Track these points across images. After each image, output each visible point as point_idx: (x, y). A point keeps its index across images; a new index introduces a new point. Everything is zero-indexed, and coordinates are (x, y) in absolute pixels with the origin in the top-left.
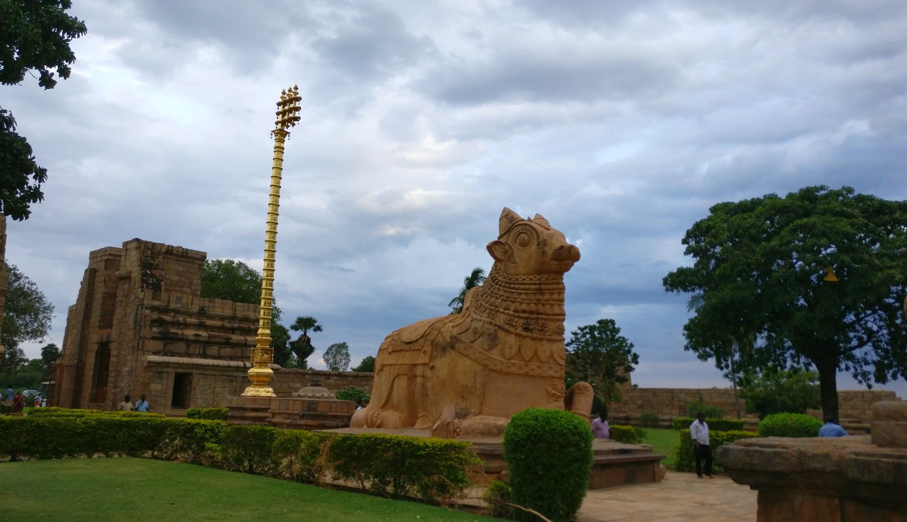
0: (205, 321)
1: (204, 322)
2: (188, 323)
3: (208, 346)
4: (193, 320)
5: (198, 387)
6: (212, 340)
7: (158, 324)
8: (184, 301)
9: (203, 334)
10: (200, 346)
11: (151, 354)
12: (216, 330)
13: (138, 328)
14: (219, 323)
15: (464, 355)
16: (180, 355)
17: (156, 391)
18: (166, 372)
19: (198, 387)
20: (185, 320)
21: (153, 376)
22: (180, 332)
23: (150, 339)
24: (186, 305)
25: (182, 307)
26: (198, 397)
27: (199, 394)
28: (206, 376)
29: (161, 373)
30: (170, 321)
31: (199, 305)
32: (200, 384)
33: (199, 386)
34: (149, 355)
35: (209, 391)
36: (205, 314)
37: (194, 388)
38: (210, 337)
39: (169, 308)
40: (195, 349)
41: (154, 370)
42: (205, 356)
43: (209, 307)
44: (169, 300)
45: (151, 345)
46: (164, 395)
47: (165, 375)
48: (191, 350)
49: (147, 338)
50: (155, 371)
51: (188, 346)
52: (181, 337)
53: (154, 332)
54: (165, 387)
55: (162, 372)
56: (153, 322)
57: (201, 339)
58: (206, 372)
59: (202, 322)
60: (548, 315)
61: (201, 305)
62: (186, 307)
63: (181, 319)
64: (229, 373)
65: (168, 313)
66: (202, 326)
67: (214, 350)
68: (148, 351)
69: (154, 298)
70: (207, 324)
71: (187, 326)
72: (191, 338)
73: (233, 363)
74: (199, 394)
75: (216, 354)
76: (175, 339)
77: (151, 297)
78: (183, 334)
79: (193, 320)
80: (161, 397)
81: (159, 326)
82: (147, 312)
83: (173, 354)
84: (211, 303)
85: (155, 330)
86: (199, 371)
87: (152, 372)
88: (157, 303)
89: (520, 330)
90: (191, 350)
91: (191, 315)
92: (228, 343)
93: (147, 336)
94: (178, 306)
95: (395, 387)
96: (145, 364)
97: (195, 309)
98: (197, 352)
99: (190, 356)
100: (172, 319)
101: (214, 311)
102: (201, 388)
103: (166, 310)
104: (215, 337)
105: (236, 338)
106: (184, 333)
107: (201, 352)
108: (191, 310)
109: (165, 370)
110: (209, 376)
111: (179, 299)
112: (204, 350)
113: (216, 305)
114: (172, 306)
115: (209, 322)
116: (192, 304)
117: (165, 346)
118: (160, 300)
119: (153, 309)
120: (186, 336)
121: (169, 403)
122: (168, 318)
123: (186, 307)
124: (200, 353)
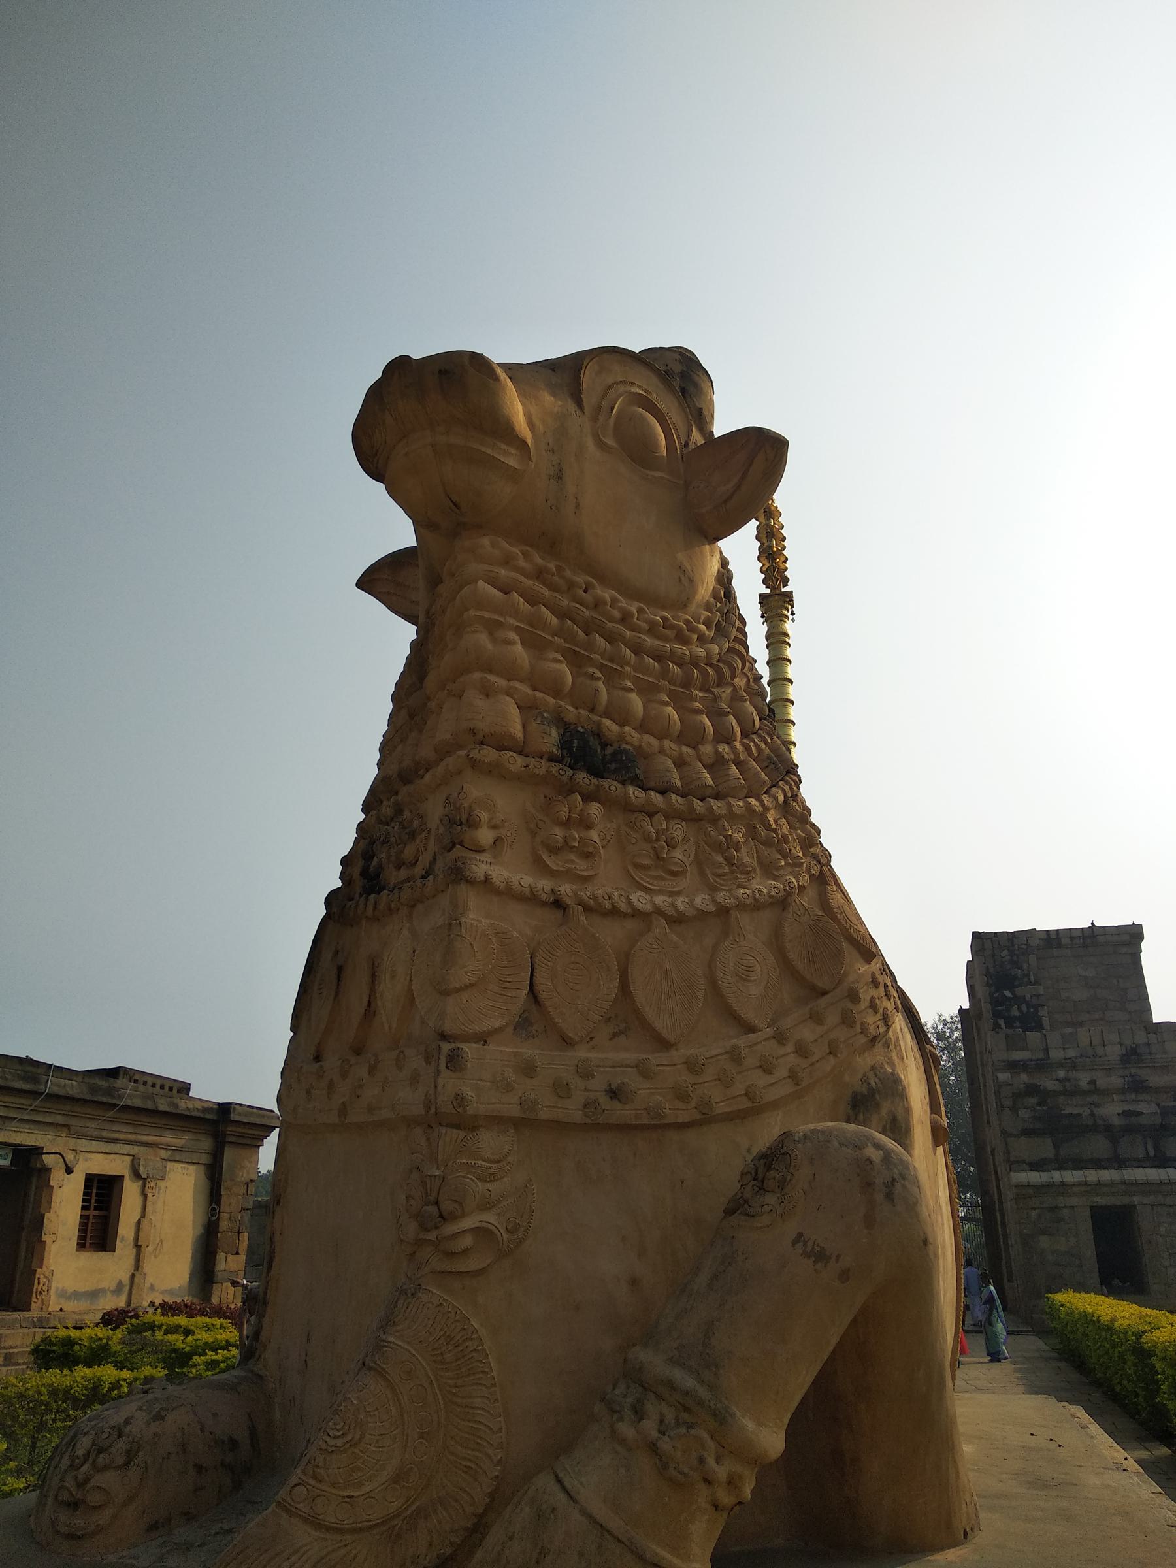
7: (1033, 1101)
11: (1027, 1167)
16: (1098, 1164)
20: (1093, 1082)
25: (1082, 1056)
26: (1167, 1263)
29: (1054, 1209)
43: (1148, 1044)
57: (1144, 1121)
72: (1116, 1122)
78: (1092, 1114)
79: (1116, 1081)
83: (1079, 1164)
88: (1019, 1055)
94: (1071, 1053)
97: (1114, 1052)
98: (1141, 1153)
99: (1120, 1163)
103: (1043, 1065)
107: (1152, 1153)
112: (1156, 1147)
114: (1056, 1055)
117: (1056, 1146)
118: (1025, 1048)
122: (1049, 1084)
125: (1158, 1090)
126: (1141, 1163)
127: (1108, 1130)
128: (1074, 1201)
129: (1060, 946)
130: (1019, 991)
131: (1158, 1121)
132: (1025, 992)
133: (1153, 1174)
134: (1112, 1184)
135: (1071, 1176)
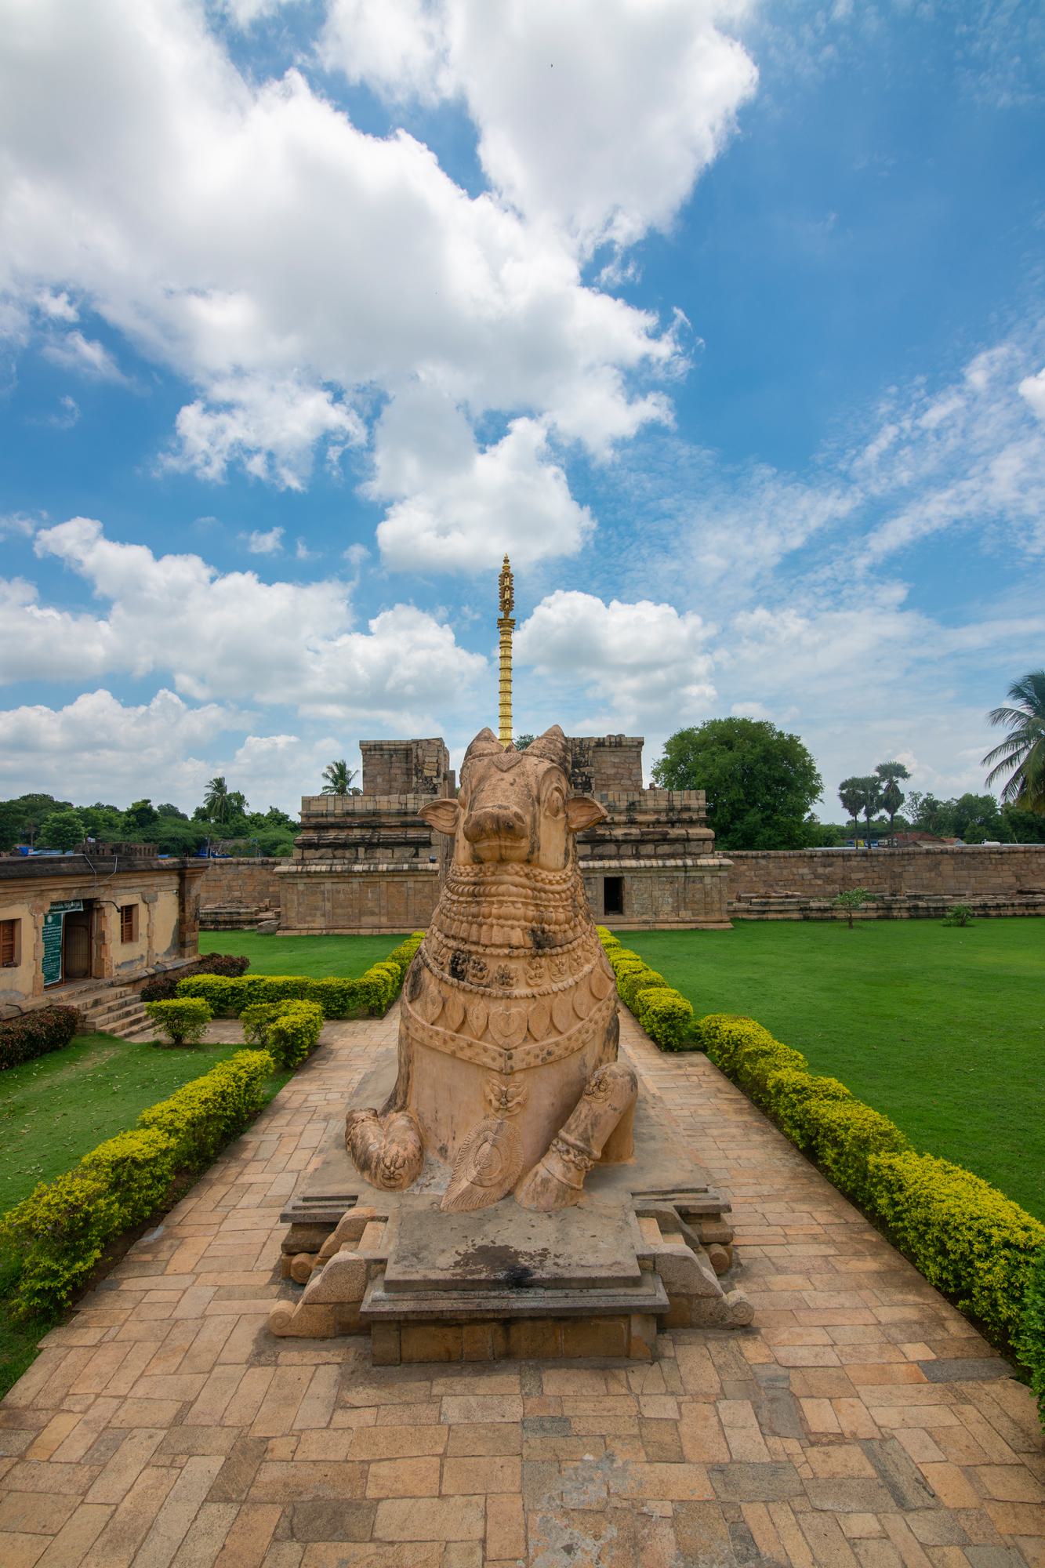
8: (610, 798)
14: (652, 818)
16: (610, 858)
22: (608, 833)
35: (646, 896)
40: (627, 849)
42: (637, 856)
52: (608, 838)
57: (633, 838)
61: (631, 799)
64: (668, 874)
66: (632, 822)
67: (649, 849)
73: (671, 863)
75: (653, 853)
76: (603, 841)
79: (623, 818)
83: (601, 858)
91: (620, 813)
92: (665, 839)
97: (623, 805)
99: (619, 857)
104: (648, 833)
105: (677, 832)
109: (592, 875)
115: (640, 818)
117: (592, 849)
121: (602, 910)
125: (641, 823)
126: (629, 857)
127: (617, 841)
128: (597, 875)
129: (604, 746)
130: (583, 770)
132: (585, 770)
133: (633, 863)
134: (616, 868)
135: (598, 864)
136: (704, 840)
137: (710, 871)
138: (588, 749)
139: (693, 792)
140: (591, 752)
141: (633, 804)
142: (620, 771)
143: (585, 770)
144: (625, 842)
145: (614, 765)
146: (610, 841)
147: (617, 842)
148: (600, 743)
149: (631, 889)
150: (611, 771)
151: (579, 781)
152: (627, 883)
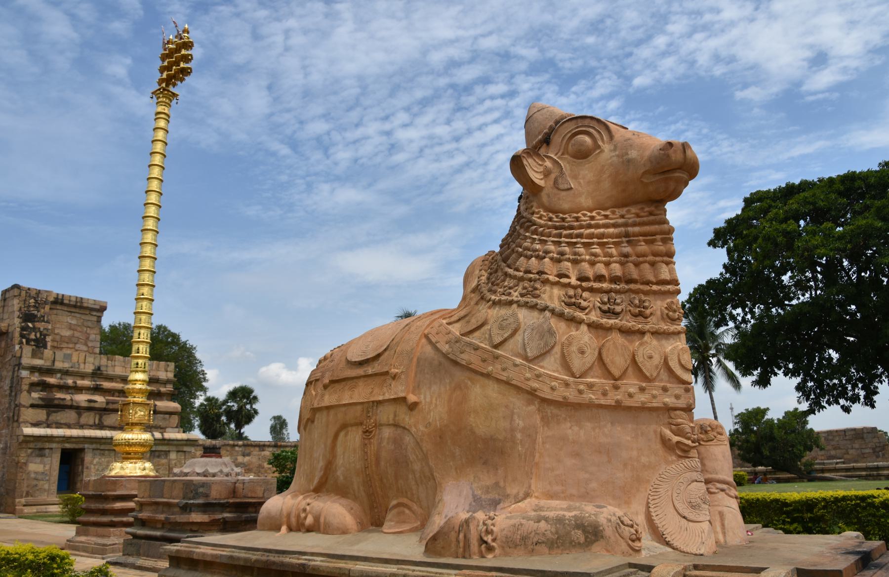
0: (102, 383)
1: (100, 385)
2: (80, 386)
3: (105, 414)
4: (87, 383)
5: (92, 466)
6: (111, 406)
8: (75, 358)
9: (100, 399)
10: (95, 414)
11: (29, 425)
12: (117, 394)
13: (13, 394)
15: (482, 374)
16: (69, 426)
17: (36, 473)
18: (48, 448)
19: (92, 466)
21: (32, 453)
22: (68, 397)
23: (27, 408)
24: (77, 364)
27: (93, 474)
28: (102, 452)
30: (56, 384)
31: (93, 364)
32: (95, 462)
33: (95, 465)
34: (27, 427)
36: (101, 374)
37: (87, 468)
38: (108, 403)
39: (54, 368)
41: (32, 445)
44: (54, 358)
45: (28, 414)
46: (47, 478)
47: (47, 451)
48: (83, 420)
49: (24, 406)
50: (33, 447)
51: (80, 415)
52: (69, 403)
53: (33, 399)
54: (47, 467)
55: (44, 449)
56: (33, 386)
57: (96, 405)
58: (102, 447)
59: (97, 385)
60: (648, 283)
61: (97, 364)
62: (77, 366)
63: (70, 382)
65: (53, 373)
66: (97, 390)
68: (26, 422)
69: (34, 355)
70: (104, 387)
71: (78, 389)
74: (93, 474)
76: (62, 407)
77: (30, 355)
78: (72, 400)
80: (43, 480)
81: (41, 391)
82: (24, 373)
83: (59, 425)
84: (109, 362)
85: (35, 395)
86: (94, 446)
87: (30, 448)
89: (594, 317)
90: (83, 420)
91: (83, 376)
93: (23, 403)
95: (339, 449)
96: (21, 438)
98: (91, 422)
99: (82, 427)
100: (59, 381)
101: (114, 371)
102: (97, 467)
106: (73, 399)
107: (97, 422)
108: (84, 370)
109: (47, 445)
110: (106, 452)
111: (68, 357)
112: (100, 420)
113: (117, 363)
115: (107, 385)
116: (85, 363)
117: (48, 415)
119: (33, 369)
120: (77, 402)
121: (54, 487)
123: (77, 366)
124: (95, 423)
126: (91, 427)
131: (104, 406)
136: (171, 413)
137: (177, 445)
138: (46, 303)
139: (162, 363)
140: (47, 307)
141: (99, 369)
142: (77, 334)
143: (41, 326)
144: (89, 409)
145: (70, 327)
146: (71, 407)
147: (77, 408)
148: (59, 302)
149: (91, 463)
150: (67, 333)
151: (32, 336)
152: (88, 457)
